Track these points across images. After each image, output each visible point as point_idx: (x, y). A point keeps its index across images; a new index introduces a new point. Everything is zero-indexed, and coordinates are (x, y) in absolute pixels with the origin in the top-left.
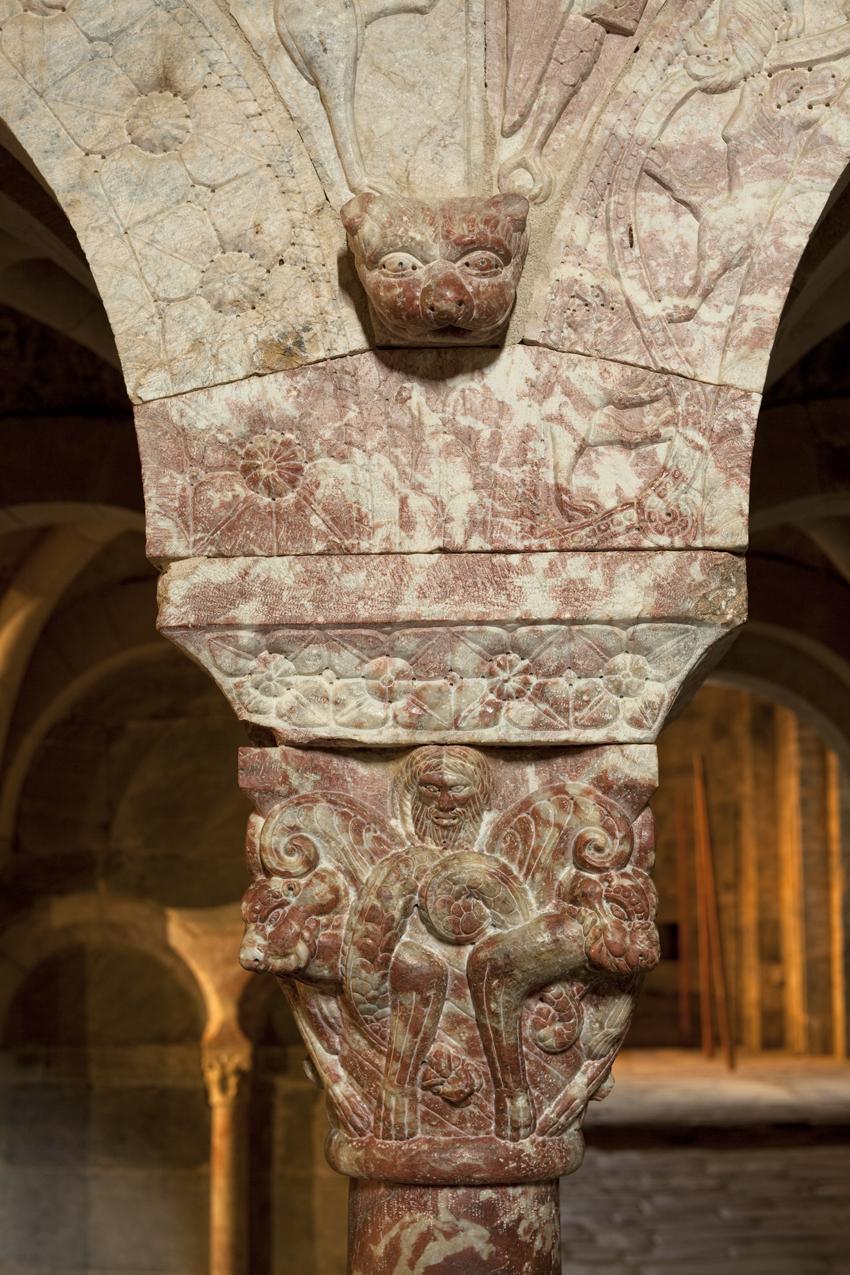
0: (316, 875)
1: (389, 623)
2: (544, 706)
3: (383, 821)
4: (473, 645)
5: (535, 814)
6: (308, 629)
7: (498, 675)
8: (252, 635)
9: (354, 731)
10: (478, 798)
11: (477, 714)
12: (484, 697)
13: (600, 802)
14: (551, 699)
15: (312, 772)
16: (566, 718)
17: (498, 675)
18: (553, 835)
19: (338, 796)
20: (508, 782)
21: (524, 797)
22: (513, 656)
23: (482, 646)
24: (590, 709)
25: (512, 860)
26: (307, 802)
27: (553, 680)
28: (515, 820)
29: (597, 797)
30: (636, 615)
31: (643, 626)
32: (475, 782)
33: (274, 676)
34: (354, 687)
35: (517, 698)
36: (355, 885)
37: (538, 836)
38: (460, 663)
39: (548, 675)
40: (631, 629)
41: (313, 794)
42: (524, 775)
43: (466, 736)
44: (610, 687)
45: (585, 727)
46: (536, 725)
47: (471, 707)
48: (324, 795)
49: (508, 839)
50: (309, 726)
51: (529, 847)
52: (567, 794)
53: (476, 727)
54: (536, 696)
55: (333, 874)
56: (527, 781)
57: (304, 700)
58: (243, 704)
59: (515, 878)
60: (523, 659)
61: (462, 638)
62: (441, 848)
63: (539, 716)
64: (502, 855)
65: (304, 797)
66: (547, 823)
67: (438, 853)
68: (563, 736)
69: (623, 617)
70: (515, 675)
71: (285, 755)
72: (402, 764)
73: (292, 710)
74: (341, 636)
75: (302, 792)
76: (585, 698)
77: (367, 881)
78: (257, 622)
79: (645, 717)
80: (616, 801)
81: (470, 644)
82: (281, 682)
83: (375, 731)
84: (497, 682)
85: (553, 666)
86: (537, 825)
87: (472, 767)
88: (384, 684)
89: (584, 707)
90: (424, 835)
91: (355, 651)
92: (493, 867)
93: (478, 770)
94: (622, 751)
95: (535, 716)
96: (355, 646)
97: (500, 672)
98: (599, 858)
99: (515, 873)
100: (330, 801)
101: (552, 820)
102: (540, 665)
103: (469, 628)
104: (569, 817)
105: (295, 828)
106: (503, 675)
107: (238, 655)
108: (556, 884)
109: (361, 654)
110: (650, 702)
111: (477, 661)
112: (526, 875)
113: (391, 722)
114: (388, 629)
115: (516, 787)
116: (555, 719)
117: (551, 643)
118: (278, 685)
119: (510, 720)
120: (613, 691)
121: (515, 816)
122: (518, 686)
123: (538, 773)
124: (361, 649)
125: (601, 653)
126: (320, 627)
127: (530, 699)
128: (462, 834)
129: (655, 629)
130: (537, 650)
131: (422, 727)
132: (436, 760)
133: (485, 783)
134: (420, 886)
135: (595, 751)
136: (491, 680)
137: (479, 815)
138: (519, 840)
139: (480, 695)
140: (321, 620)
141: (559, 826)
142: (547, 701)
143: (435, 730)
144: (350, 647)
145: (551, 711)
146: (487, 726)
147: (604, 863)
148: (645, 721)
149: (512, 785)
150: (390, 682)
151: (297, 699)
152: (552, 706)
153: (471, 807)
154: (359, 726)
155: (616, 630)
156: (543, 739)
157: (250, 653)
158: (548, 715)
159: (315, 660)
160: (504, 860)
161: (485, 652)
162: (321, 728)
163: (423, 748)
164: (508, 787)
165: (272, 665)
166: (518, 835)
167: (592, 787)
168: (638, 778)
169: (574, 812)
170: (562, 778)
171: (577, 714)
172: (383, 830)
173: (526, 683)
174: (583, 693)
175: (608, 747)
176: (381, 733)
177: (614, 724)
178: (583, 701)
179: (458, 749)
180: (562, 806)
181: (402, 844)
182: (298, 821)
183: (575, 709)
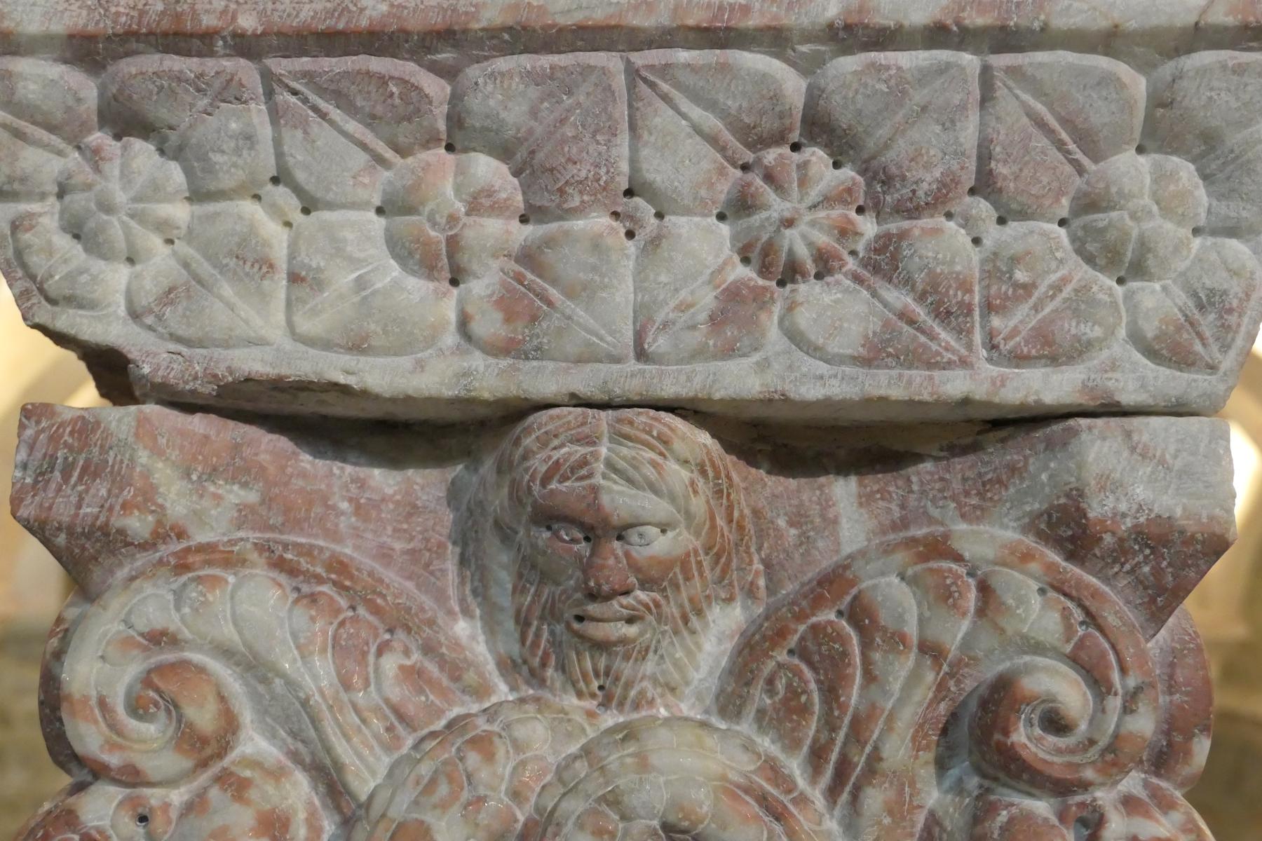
0: (223, 779)
1: (448, 36)
2: (898, 298)
3: (431, 623)
4: (696, 113)
5: (860, 614)
6: (212, 54)
7: (767, 207)
8: (55, 71)
9: (347, 360)
10: (699, 563)
11: (703, 316)
12: (721, 270)
13: (1058, 586)
14: (920, 278)
15: (233, 480)
16: (963, 332)
17: (767, 207)
18: (914, 678)
19: (307, 551)
20: (782, 522)
21: (824, 562)
22: (817, 156)
23: (724, 114)
24: (1036, 308)
25: (792, 745)
26: (209, 563)
27: (926, 222)
28: (802, 628)
29: (1051, 567)
30: (1191, 19)
31: (1206, 57)
32: (689, 516)
33: (121, 197)
34: (349, 235)
35: (819, 276)
36: (338, 808)
37: (870, 677)
38: (657, 171)
39: (911, 210)
40: (1167, 69)
41: (233, 542)
42: (826, 504)
43: (672, 386)
44: (1091, 247)
45: (1019, 359)
46: (871, 358)
47: (683, 294)
48: (261, 547)
49: (780, 685)
50: (227, 344)
51: (843, 707)
52: (958, 558)
53: (698, 354)
54: (876, 269)
55: (277, 774)
56: (836, 521)
57: (205, 269)
58: (33, 278)
59: (802, 800)
60: (837, 165)
61: (665, 87)
62: (591, 704)
63: (886, 324)
64: (761, 729)
65: (202, 548)
66: (897, 640)
67: (579, 718)
68: (955, 385)
69: (1154, 21)
70: (814, 207)
71: (142, 421)
72: (488, 466)
73: (169, 295)
74: (309, 76)
75: (201, 537)
76: (1021, 276)
77: (372, 797)
78: (58, 27)
79: (1200, 336)
80: (1106, 580)
81: (685, 105)
82: (132, 216)
83: (406, 362)
84: (762, 227)
85: (927, 180)
86: (866, 645)
87: (685, 474)
88: (434, 224)
89: (1018, 300)
90: (544, 664)
91: (352, 126)
92: (741, 765)
93: (700, 483)
94: (1128, 434)
95: (875, 325)
96: (351, 109)
97: (770, 195)
98: (1059, 751)
99: (801, 783)
100: (279, 564)
101: (912, 630)
102: (888, 182)
103: (683, 56)
104: (965, 625)
105: (158, 638)
106: (777, 206)
107: (18, 134)
108: (920, 819)
109: (369, 137)
110: (1212, 292)
111: (705, 165)
112: (833, 793)
113: (450, 338)
114: (446, 56)
115: (804, 539)
116: (933, 337)
117: (924, 109)
118: (133, 224)
119: (795, 337)
120: (1101, 261)
121: (800, 617)
122: (823, 239)
123: (865, 500)
124: (371, 120)
125: (1072, 146)
126: (245, 46)
127: (857, 279)
128: (649, 666)
129: (1240, 70)
130: (883, 133)
131: (540, 353)
132: (581, 450)
133: (720, 522)
134: (521, 818)
135: (1039, 434)
136: (744, 223)
137: (699, 613)
138: (813, 686)
139: (712, 262)
140: (248, 22)
141: (931, 650)
142: (908, 283)
143: (580, 360)
144: (336, 114)
145: (921, 312)
146: (729, 352)
147: (1077, 767)
148: (1198, 347)
149: (793, 531)
150: (453, 219)
151: (186, 265)
152: (921, 298)
153: (676, 587)
154: (358, 346)
155: (1122, 70)
156: (896, 393)
157: (52, 128)
158: (911, 322)
159: (237, 151)
160: (766, 744)
161: (727, 137)
162: (255, 351)
163: (543, 416)
164: (779, 535)
165: (113, 169)
166: (808, 674)
167: (1030, 541)
168: (1179, 512)
169: (981, 612)
170: (935, 512)
171: (996, 322)
172: (429, 649)
173: (845, 232)
174: (1015, 260)
175: (1084, 422)
176: (420, 366)
177: (1105, 354)
178: (1017, 286)
179: (643, 417)
180: (946, 596)
181: (481, 691)
182: (171, 620)
183: (989, 308)
